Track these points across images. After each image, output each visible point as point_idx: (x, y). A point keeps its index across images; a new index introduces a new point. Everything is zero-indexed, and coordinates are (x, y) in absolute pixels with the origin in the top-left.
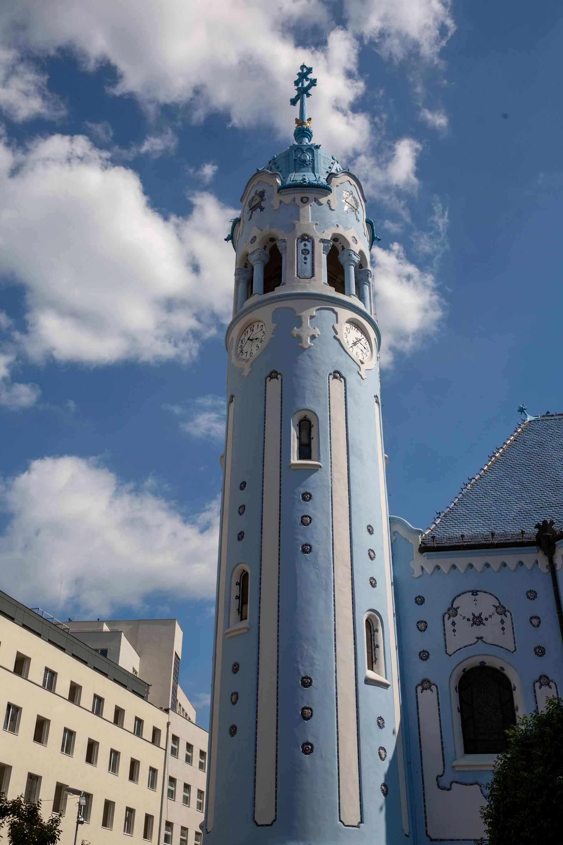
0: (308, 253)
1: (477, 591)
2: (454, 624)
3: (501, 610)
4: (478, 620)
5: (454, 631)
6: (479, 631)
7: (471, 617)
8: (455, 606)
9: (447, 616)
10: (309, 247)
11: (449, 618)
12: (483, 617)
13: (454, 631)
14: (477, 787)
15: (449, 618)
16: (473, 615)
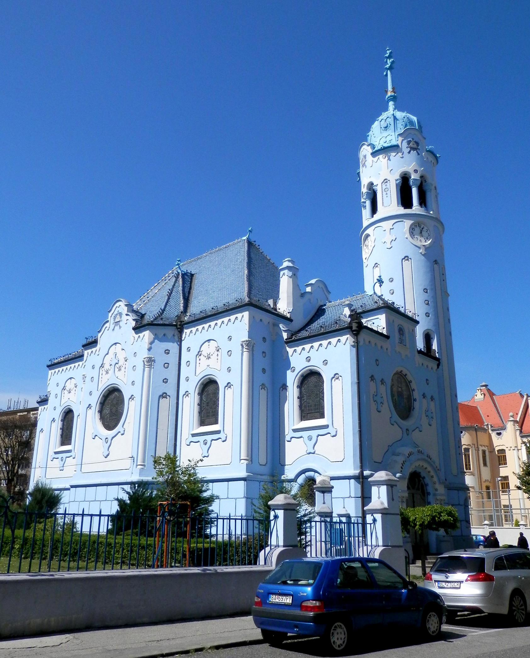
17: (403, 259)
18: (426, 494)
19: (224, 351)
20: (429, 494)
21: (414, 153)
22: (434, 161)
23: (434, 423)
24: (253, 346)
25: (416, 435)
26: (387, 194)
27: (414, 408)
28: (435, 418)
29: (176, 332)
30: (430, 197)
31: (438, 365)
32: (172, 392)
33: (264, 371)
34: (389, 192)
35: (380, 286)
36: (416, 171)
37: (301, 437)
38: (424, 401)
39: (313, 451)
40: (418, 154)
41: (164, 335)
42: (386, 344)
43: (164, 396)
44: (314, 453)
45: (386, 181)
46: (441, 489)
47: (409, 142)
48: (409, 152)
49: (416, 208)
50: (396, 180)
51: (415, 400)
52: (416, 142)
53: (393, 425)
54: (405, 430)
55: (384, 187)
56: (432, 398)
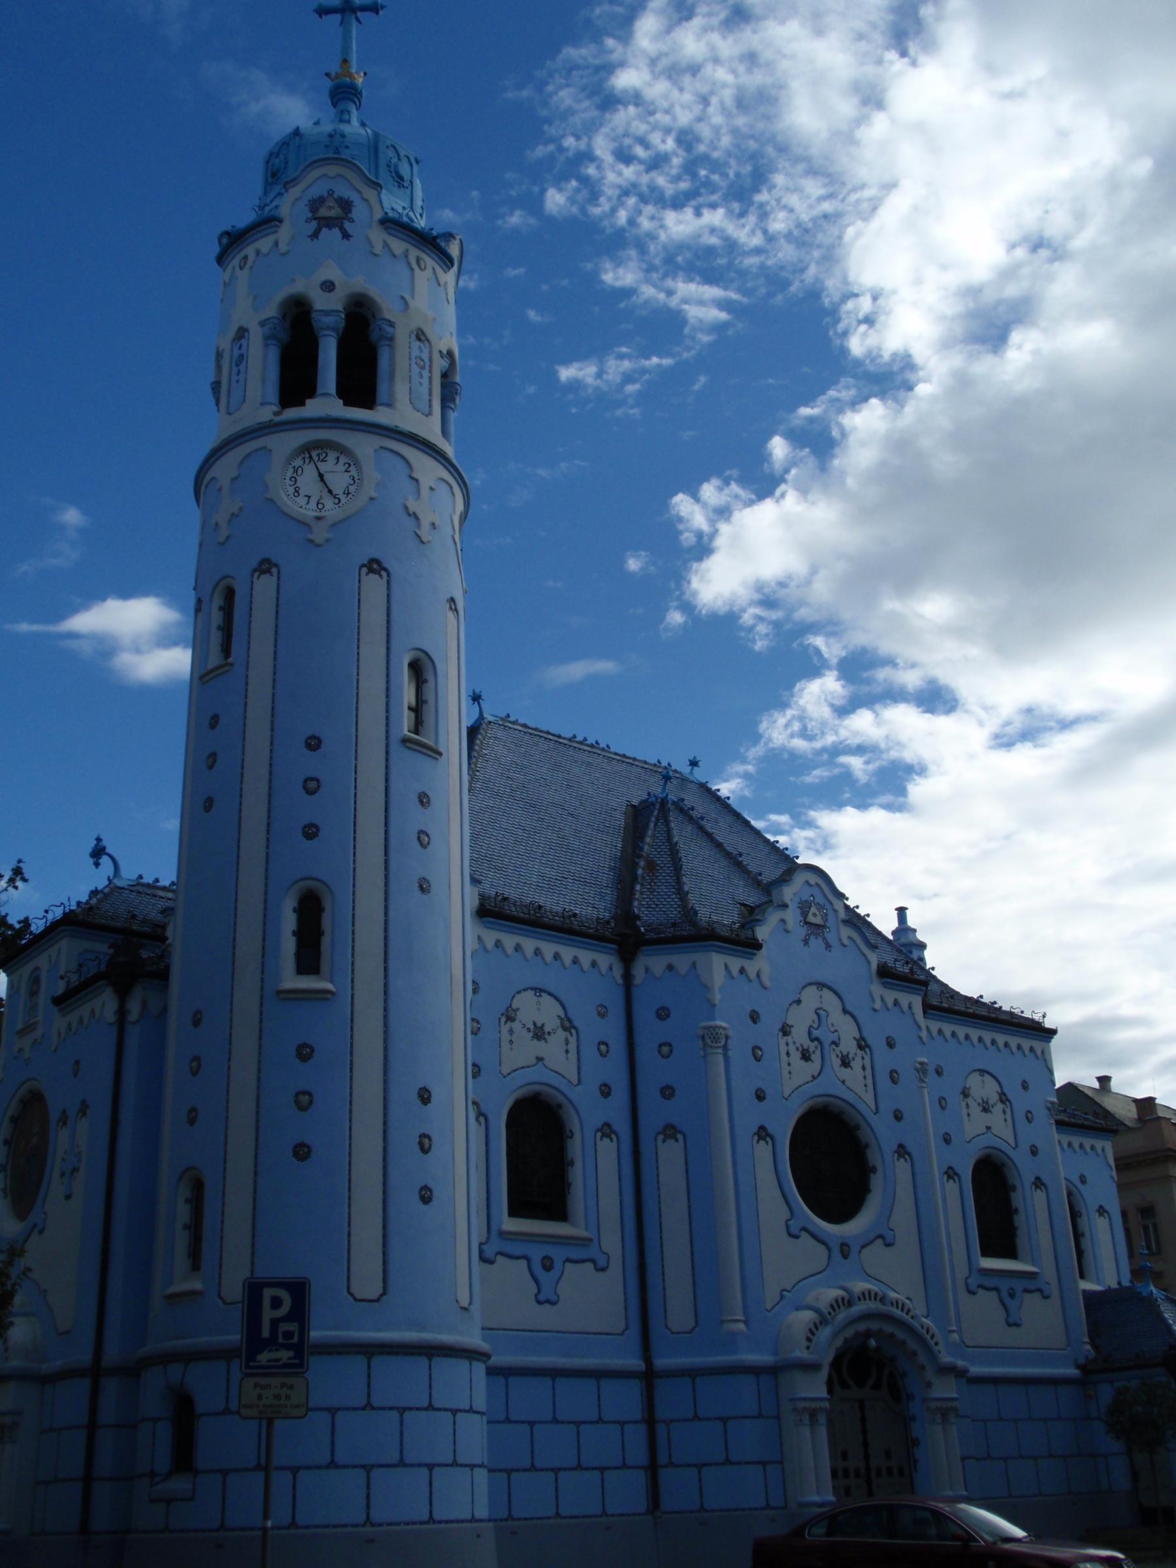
0: (423, 368)
1: (541, 990)
2: (511, 1031)
3: (568, 1024)
4: (539, 1033)
5: (511, 1042)
6: (539, 1048)
7: (532, 1027)
8: (514, 1006)
9: (503, 1019)
11: (506, 1022)
12: (546, 1029)
13: (511, 1042)
14: (524, 1263)
15: (506, 1022)
16: (535, 1024)
17: (255, 571)
21: (331, 236)
34: (242, 367)
40: (346, 236)
45: (242, 333)
47: (316, 204)
49: (326, 403)
50: (262, 324)
55: (236, 353)
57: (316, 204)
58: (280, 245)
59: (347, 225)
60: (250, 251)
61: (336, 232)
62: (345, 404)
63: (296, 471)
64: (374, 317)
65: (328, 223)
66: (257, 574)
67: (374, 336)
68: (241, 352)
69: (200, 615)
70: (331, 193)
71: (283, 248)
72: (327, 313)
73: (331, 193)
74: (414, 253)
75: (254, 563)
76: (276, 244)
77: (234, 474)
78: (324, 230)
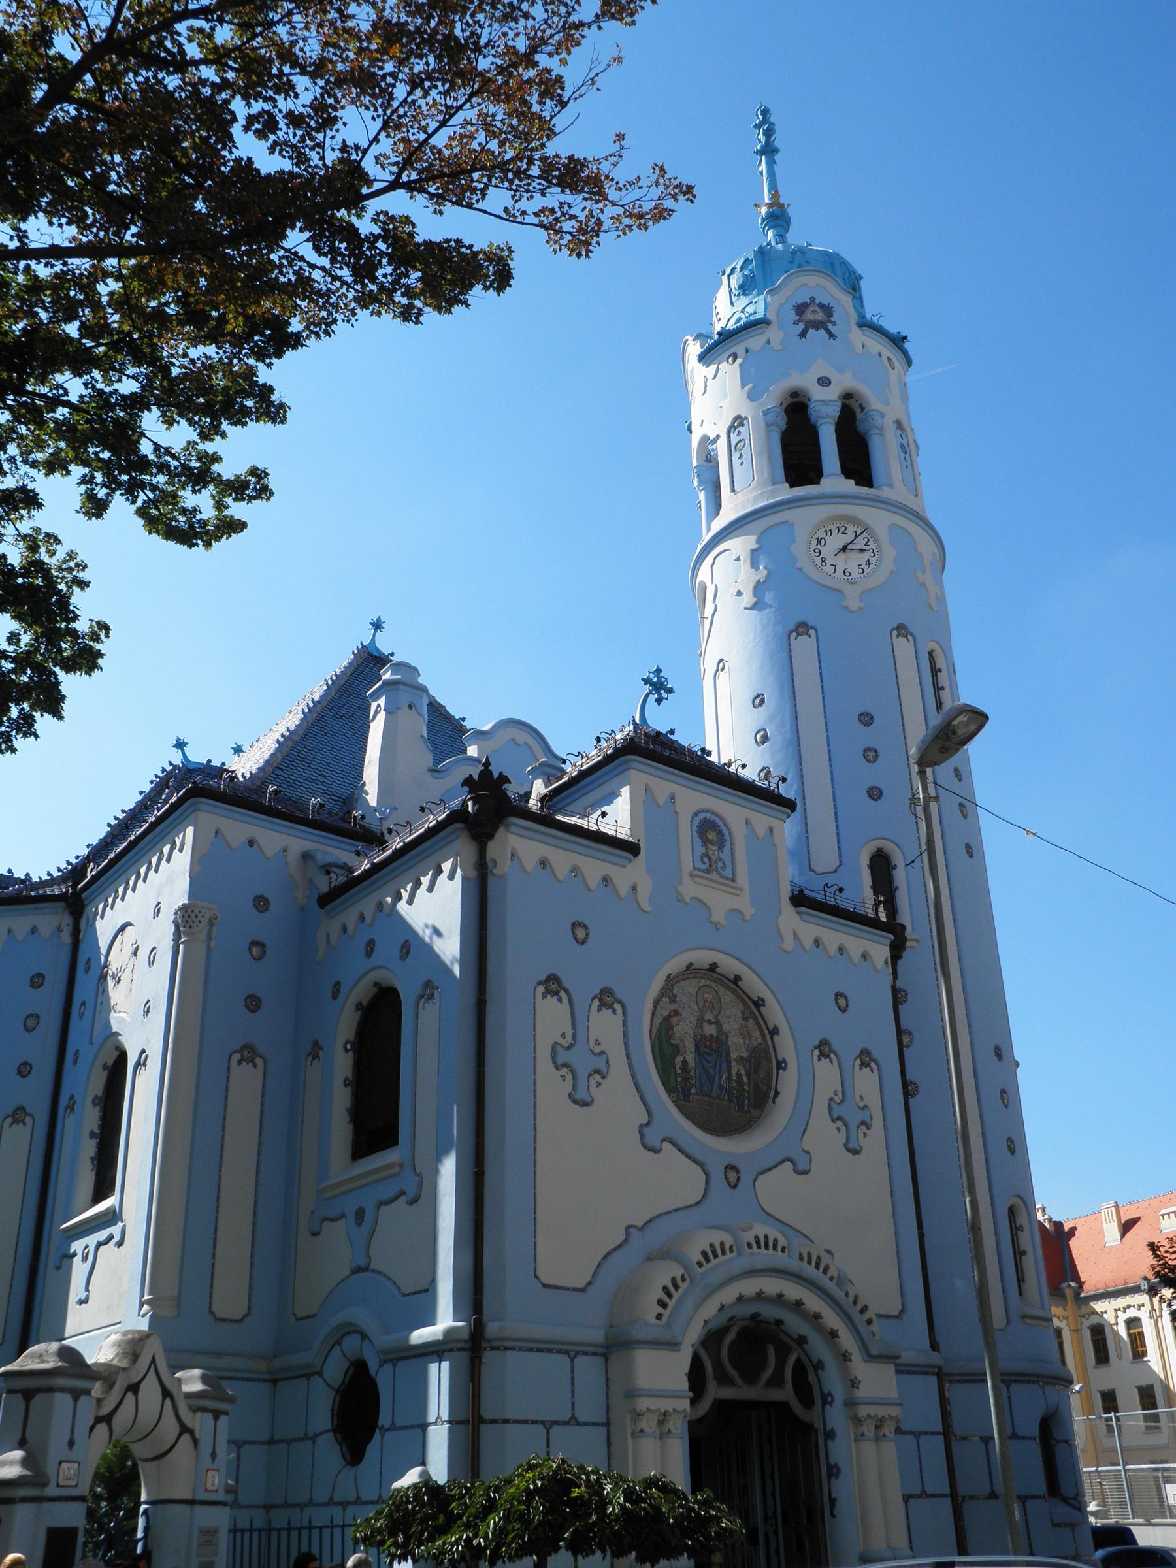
10: (905, 442)
17: (792, 632)
18: (818, 1402)
19: (143, 953)
20: (827, 1399)
22: (888, 351)
23: (873, 1142)
24: (211, 923)
25: (777, 1190)
26: (741, 457)
27: (777, 1094)
28: (877, 1123)
29: (67, 920)
30: (884, 453)
31: (897, 949)
32: (40, 1108)
33: (253, 1003)
35: (659, 701)
36: (824, 382)
37: (343, 1216)
38: (827, 1071)
39: (362, 1262)
40: (831, 335)
41: (34, 930)
42: (627, 874)
43: (19, 1115)
44: (366, 1269)
45: (738, 421)
46: (877, 1383)
47: (801, 309)
48: (803, 334)
51: (781, 1065)
52: (821, 306)
53: (656, 1151)
54: (718, 1174)
56: (866, 1058)
57: (801, 309)
58: (772, 344)
59: (830, 326)
60: (739, 349)
61: (822, 332)
62: (857, 484)
63: (819, 541)
64: (862, 408)
65: (817, 325)
66: (794, 634)
67: (861, 427)
68: (741, 437)
69: (723, 676)
70: (813, 300)
71: (775, 344)
72: (825, 403)
73: (813, 300)
74: (886, 353)
75: (792, 627)
76: (768, 342)
77: (755, 546)
78: (811, 331)
